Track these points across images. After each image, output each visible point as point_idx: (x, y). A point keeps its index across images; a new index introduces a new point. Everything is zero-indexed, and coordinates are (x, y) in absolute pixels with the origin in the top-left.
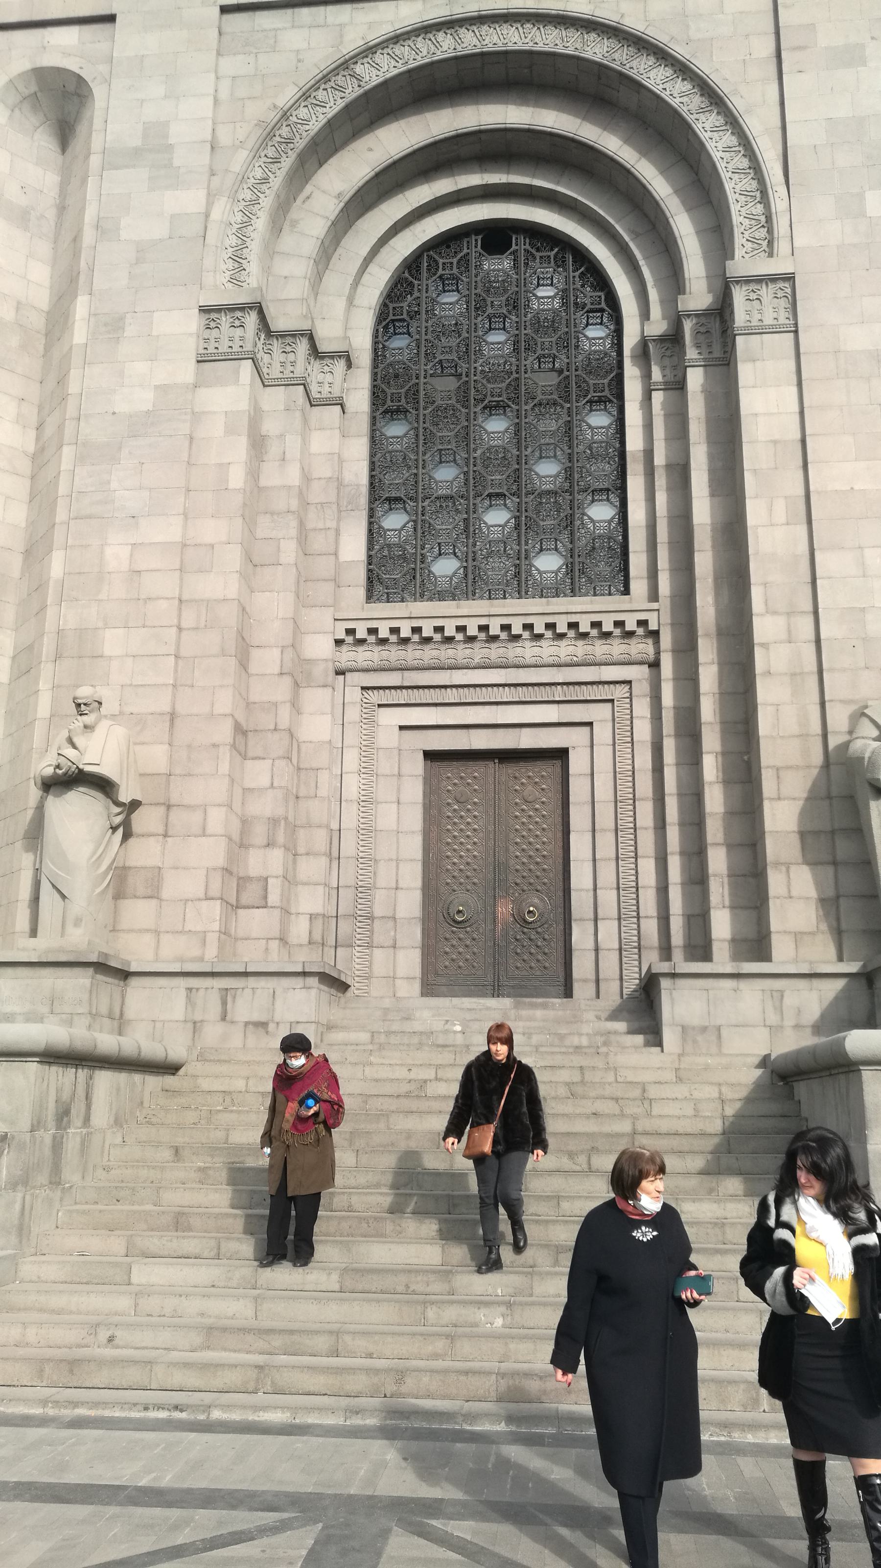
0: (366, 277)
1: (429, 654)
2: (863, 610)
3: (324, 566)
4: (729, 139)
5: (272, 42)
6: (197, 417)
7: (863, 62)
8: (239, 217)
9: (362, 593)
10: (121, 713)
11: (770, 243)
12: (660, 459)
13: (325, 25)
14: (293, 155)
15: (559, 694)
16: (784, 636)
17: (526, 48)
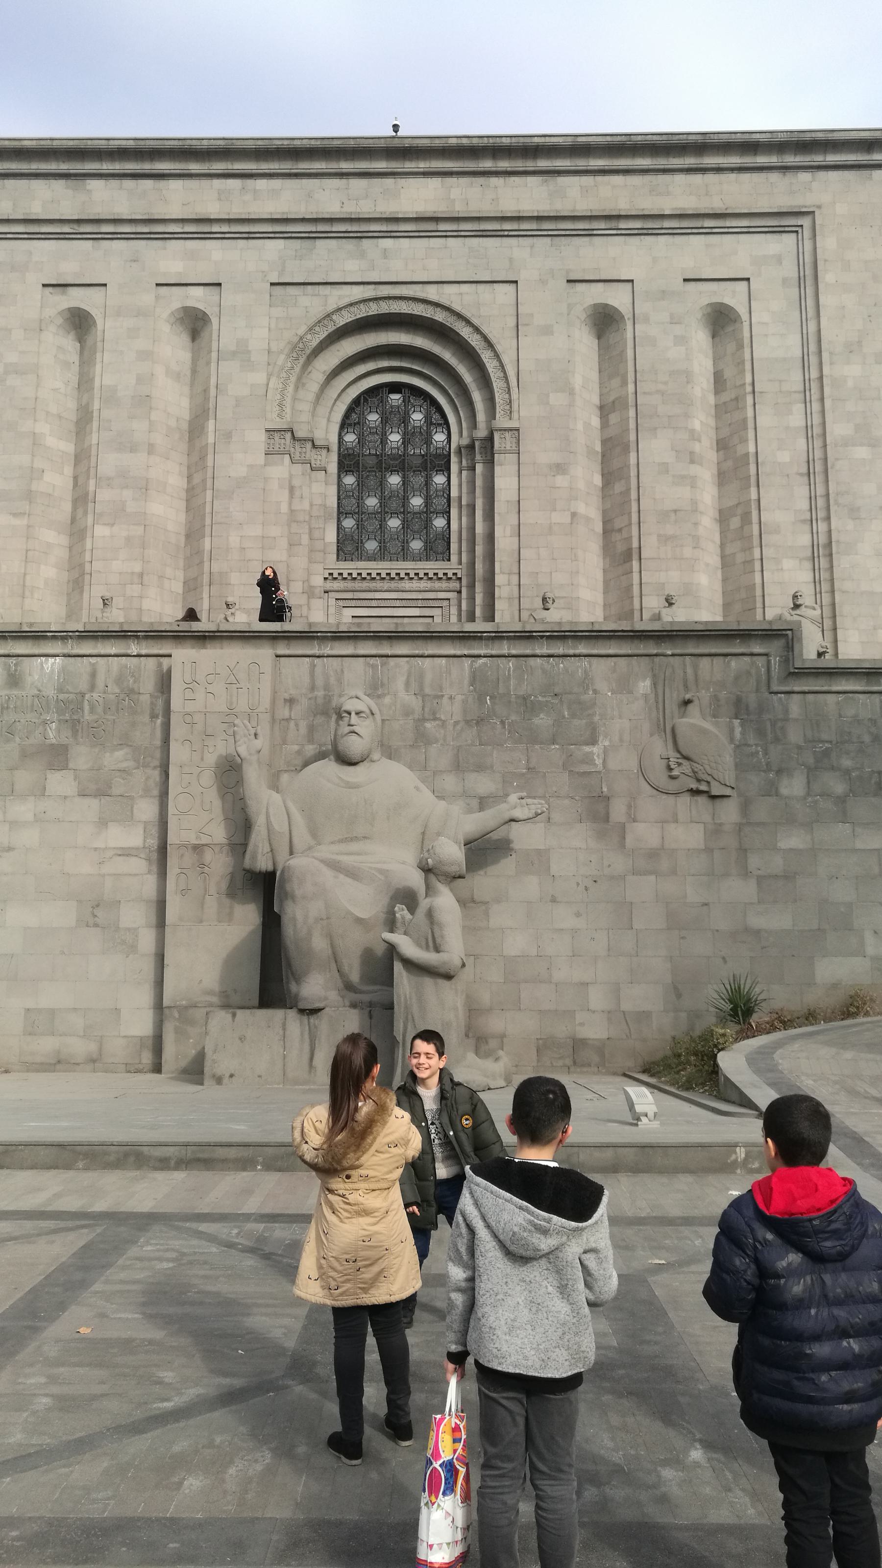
0: (335, 407)
1: (365, 585)
2: (537, 573)
3: (319, 545)
4: (495, 363)
5: (294, 301)
6: (266, 480)
7: (552, 333)
8: (281, 385)
9: (335, 556)
10: (240, 608)
11: (511, 412)
12: (464, 502)
13: (318, 295)
14: (305, 357)
15: (420, 603)
16: (507, 583)
17: (409, 312)
